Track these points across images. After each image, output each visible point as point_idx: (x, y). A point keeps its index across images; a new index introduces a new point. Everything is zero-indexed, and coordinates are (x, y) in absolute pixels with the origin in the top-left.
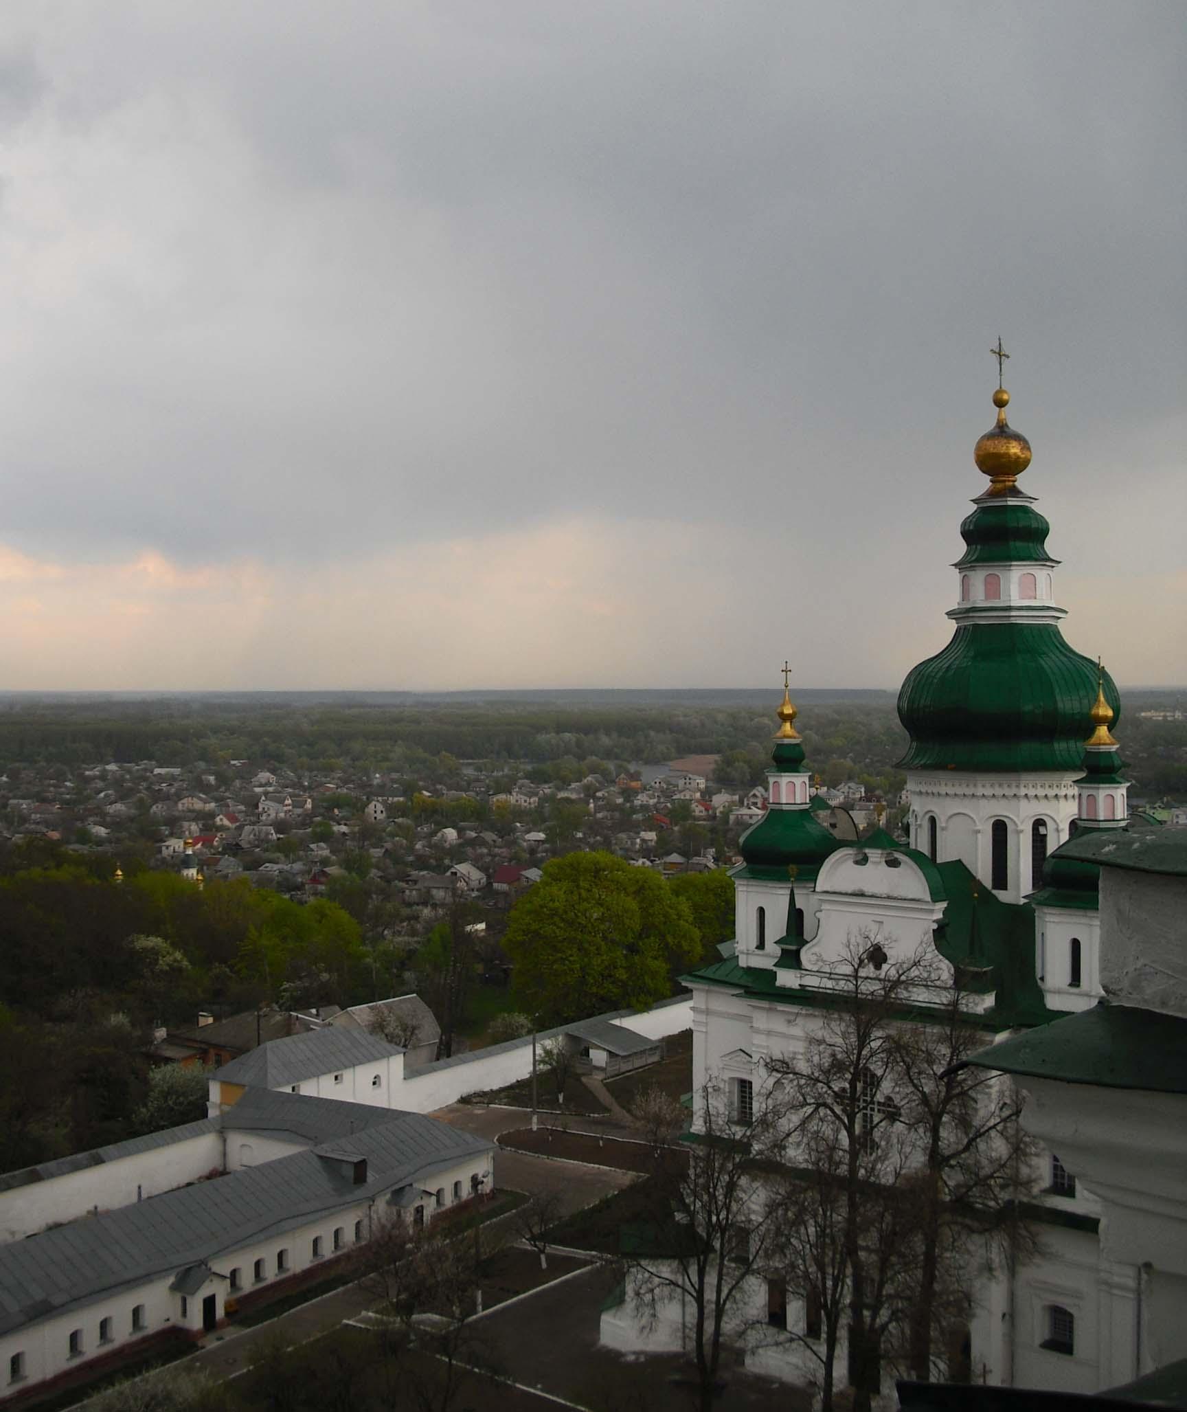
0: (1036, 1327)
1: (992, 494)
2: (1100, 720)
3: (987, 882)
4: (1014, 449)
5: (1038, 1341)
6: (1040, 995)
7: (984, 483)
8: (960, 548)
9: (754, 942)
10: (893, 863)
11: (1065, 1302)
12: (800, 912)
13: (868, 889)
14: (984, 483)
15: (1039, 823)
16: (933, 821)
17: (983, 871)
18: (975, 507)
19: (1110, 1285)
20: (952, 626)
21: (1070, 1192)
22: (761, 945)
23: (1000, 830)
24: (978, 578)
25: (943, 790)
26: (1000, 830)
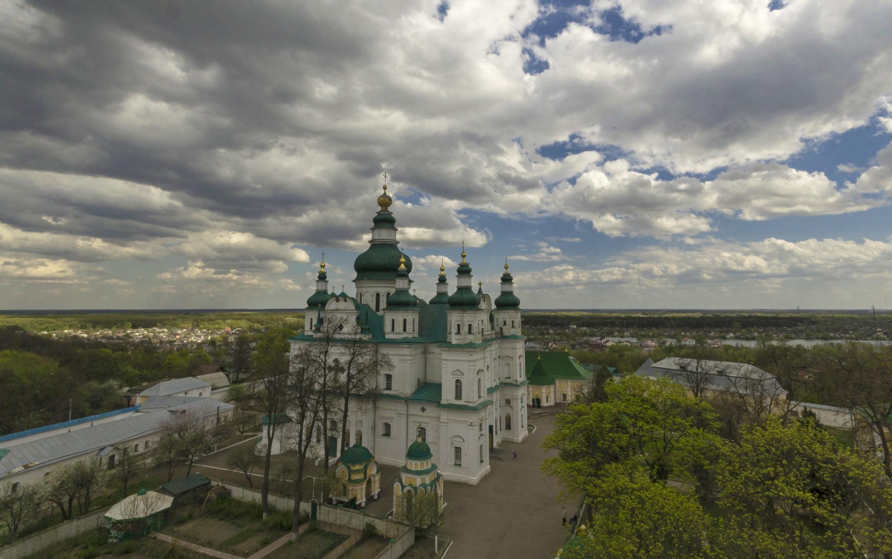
0: (381, 430)
1: (381, 211)
2: (403, 263)
3: (374, 310)
4: (387, 200)
5: (381, 434)
6: (384, 335)
7: (379, 209)
8: (373, 225)
9: (309, 329)
10: (346, 301)
11: (388, 421)
12: (322, 319)
13: (339, 309)
14: (379, 209)
15: (388, 294)
16: (361, 294)
17: (373, 306)
18: (377, 214)
19: (399, 414)
20: (370, 245)
21: (390, 389)
22: (311, 328)
23: (378, 295)
24: (376, 231)
25: (365, 285)
26: (378, 295)
